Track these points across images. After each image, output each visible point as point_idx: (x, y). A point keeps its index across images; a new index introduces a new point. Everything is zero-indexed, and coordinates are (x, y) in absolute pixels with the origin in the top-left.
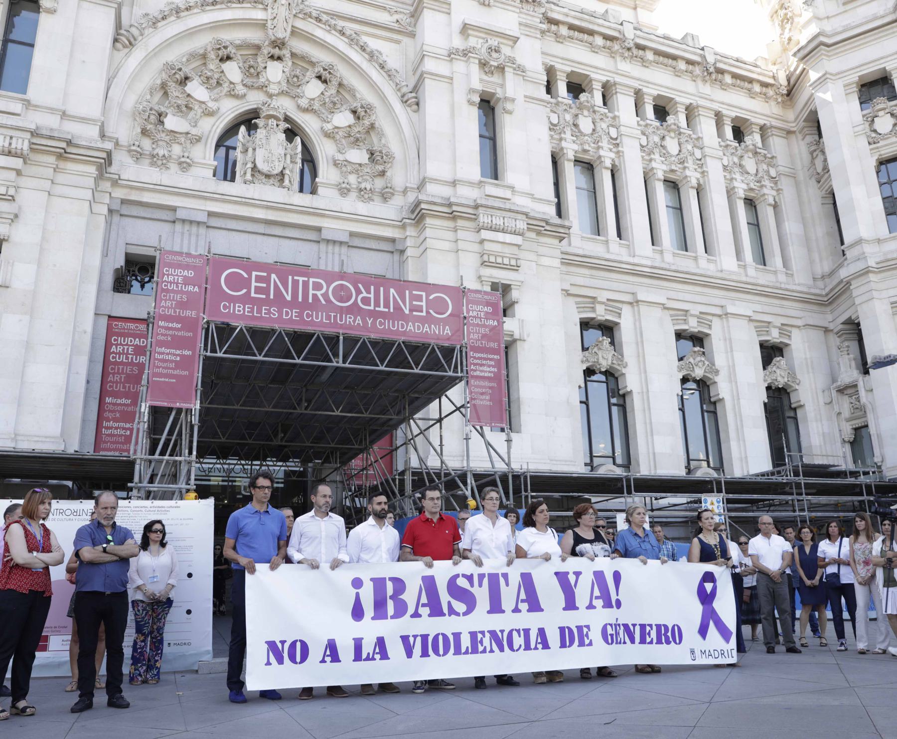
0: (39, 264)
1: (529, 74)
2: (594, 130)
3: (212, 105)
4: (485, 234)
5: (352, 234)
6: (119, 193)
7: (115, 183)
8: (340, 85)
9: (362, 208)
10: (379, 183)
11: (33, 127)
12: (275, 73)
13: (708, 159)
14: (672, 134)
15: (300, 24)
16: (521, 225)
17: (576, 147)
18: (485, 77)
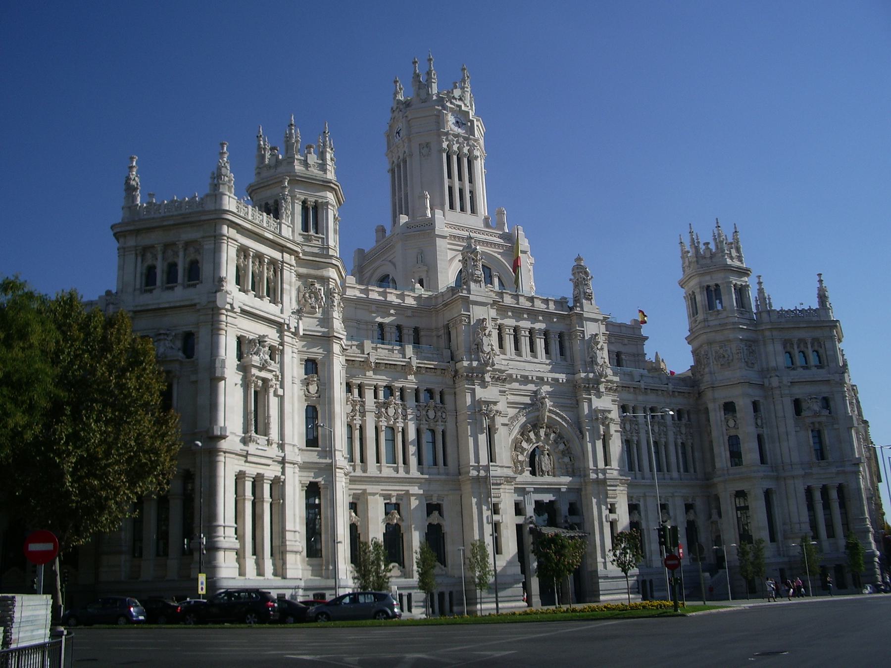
4: (608, 488)
12: (542, 432)
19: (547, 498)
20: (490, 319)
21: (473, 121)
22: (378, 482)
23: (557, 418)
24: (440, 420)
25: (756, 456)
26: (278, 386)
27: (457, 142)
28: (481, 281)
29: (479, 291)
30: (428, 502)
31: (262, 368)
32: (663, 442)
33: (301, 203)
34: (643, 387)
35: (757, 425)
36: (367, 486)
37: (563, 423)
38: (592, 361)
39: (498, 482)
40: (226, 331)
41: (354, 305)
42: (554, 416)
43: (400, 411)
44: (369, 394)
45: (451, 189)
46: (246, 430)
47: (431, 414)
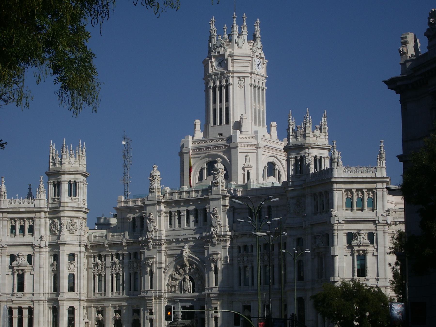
2: (248, 259)
4: (212, 299)
12: (187, 269)
19: (188, 304)
21: (227, 59)
22: (103, 301)
23: (193, 260)
26: (33, 270)
27: (218, 78)
28: (154, 191)
29: (152, 198)
30: (133, 309)
31: (18, 266)
36: (107, 303)
37: (197, 262)
39: (150, 299)
40: (1, 255)
42: (191, 259)
43: (121, 266)
44: (109, 260)
46: (13, 291)
47: (135, 265)
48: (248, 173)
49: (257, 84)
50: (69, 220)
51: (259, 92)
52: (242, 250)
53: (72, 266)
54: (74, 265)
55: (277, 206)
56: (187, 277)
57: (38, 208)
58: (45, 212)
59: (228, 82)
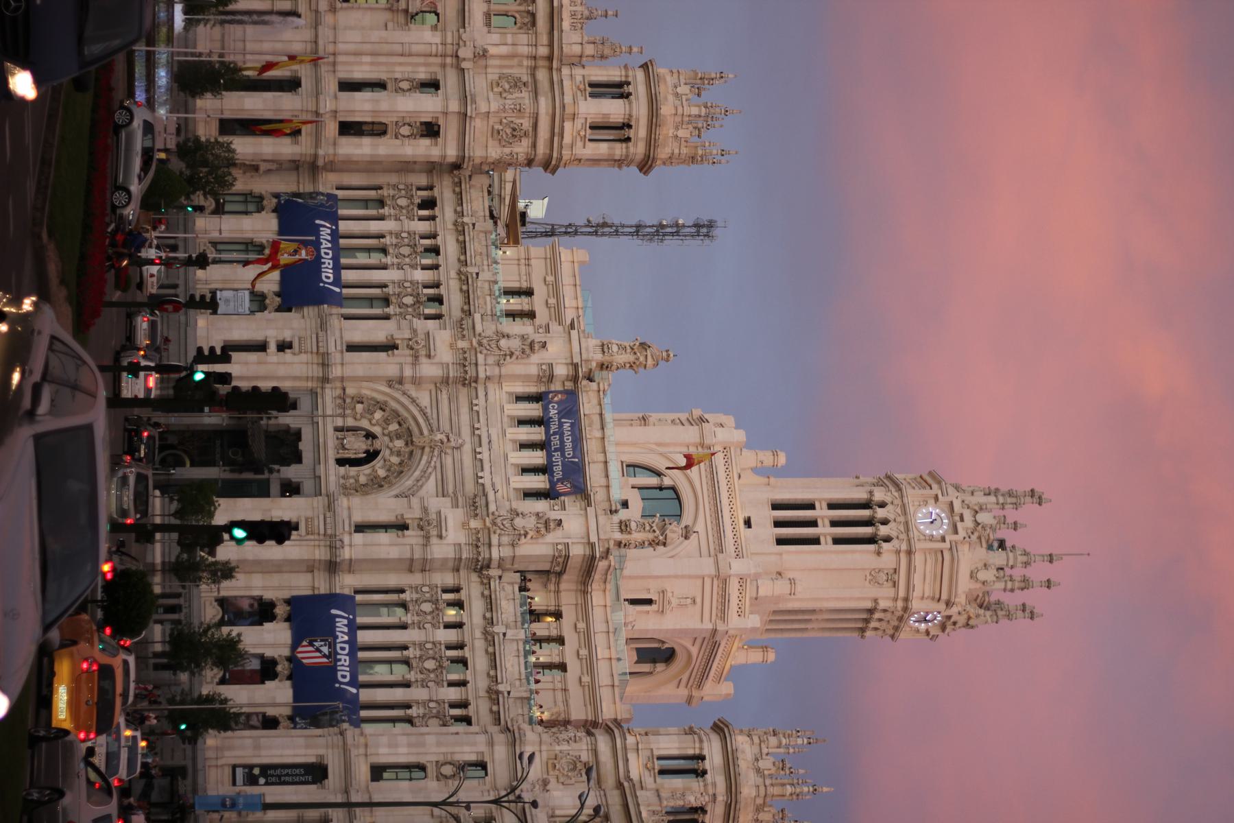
0: (278, 363)
1: (428, 547)
3: (374, 421)
4: (322, 518)
5: (320, 477)
6: (319, 390)
7: (322, 388)
8: (402, 472)
9: (332, 478)
10: (352, 491)
11: (329, 352)
12: (399, 444)
13: (426, 690)
14: (437, 664)
15: (427, 450)
16: (329, 532)
17: (408, 599)
18: (416, 524)
19: (305, 446)
20: (550, 362)
24: (402, 310)
25: (385, 755)
28: (604, 352)
32: (408, 677)
33: (623, 79)
34: (496, 629)
35: (445, 763)
38: (518, 515)
39: (320, 344)
41: (549, 256)
44: (424, 227)
45: (811, 506)
47: (408, 300)
48: (649, 602)
49: (877, 615)
50: (526, 124)
51: (856, 620)
52: (450, 596)
53: (405, 130)
54: (408, 136)
55: (565, 690)
56: (377, 444)
57: (561, 39)
58: (550, 58)
59: (885, 546)
